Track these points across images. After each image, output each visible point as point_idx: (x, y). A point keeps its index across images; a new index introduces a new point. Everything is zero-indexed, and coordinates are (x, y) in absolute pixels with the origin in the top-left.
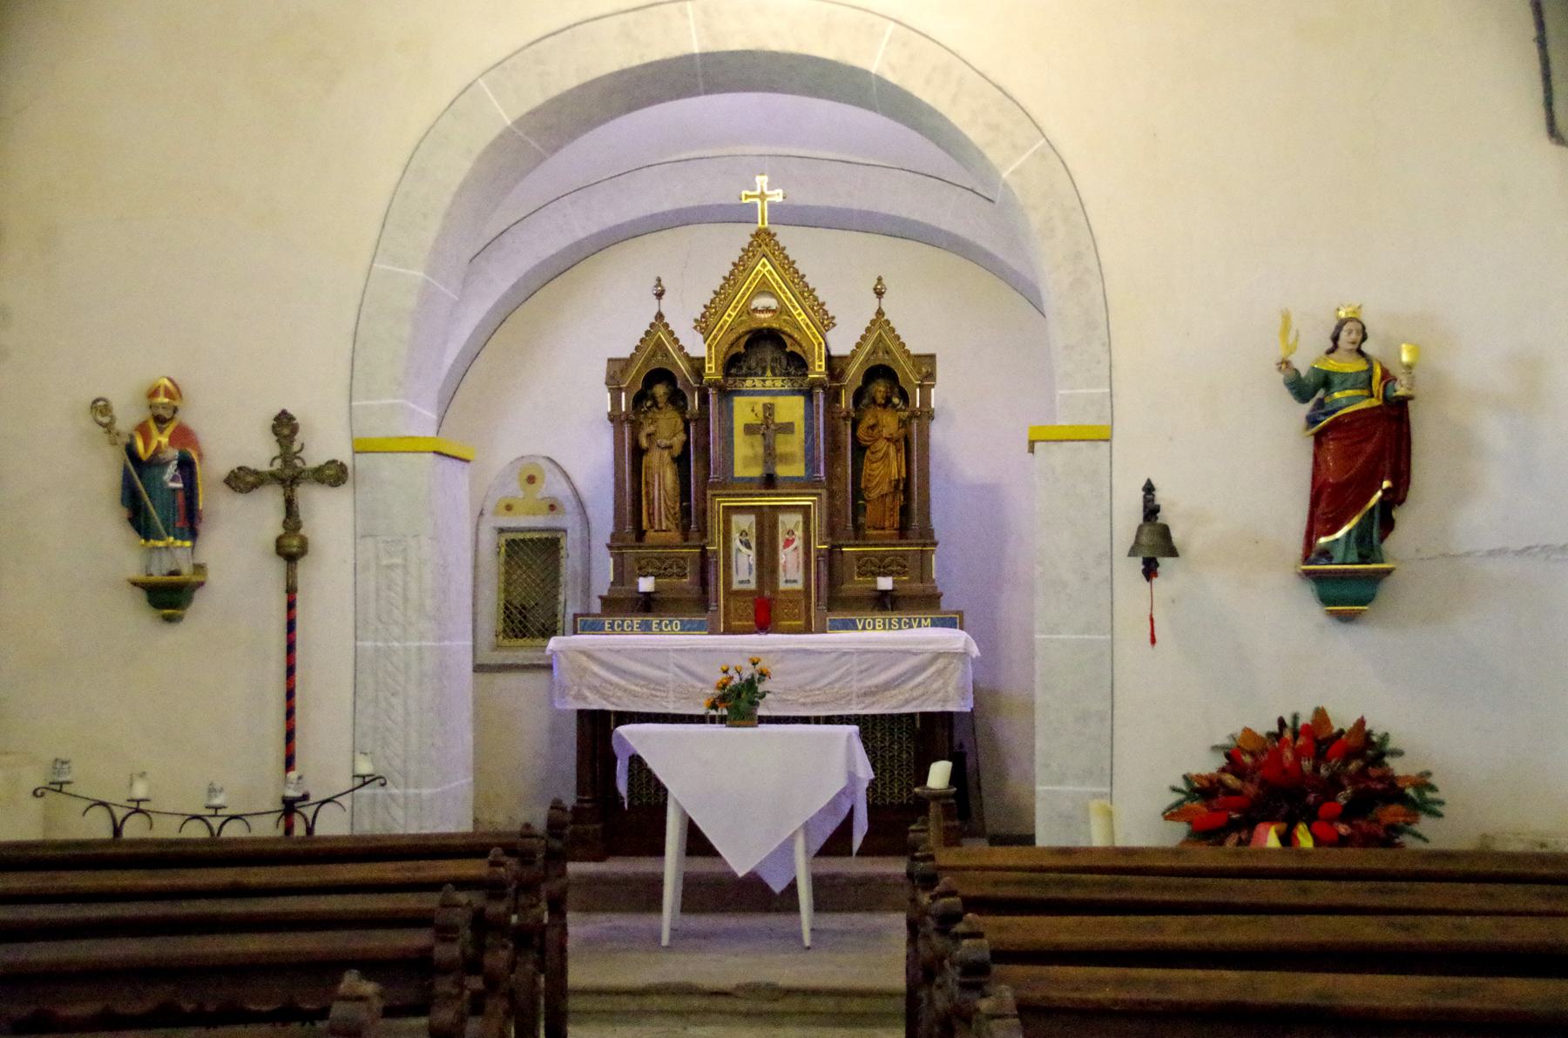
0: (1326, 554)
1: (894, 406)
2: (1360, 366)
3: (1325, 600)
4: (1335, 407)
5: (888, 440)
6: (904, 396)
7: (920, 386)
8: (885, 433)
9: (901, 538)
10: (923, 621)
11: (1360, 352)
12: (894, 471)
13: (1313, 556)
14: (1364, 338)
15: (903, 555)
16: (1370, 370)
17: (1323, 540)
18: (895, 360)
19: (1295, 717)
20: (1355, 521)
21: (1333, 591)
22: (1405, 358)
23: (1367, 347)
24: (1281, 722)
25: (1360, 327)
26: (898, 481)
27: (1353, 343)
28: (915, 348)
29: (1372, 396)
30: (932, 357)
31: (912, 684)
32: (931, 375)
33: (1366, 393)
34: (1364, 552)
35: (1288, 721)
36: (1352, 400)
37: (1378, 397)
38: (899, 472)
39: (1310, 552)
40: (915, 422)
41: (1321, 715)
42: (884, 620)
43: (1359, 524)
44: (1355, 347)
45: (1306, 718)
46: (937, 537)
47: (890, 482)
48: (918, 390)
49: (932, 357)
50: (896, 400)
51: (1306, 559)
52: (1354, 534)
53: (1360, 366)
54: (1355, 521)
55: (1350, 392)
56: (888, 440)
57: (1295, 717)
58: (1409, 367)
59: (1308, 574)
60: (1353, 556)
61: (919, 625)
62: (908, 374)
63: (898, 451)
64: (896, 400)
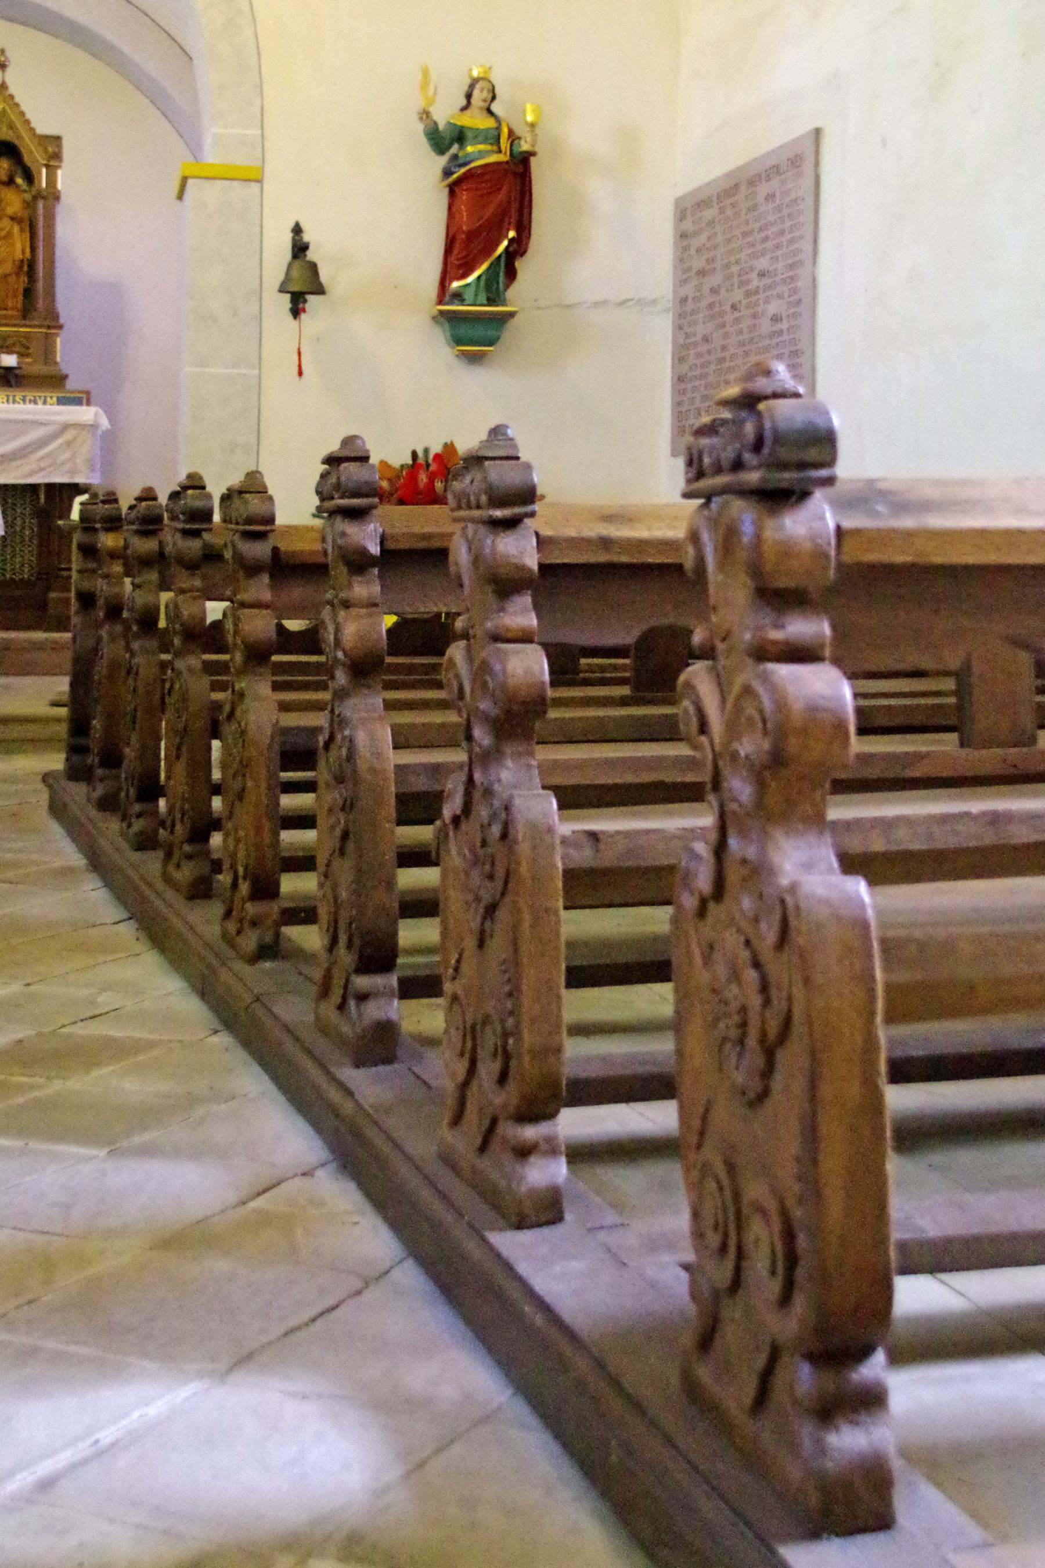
0: (458, 296)
1: (18, 186)
2: (490, 123)
3: (458, 341)
4: (468, 159)
5: (12, 219)
6: (29, 177)
7: (47, 166)
8: (10, 211)
9: (24, 318)
10: (49, 399)
11: (489, 112)
12: (18, 246)
13: (447, 298)
14: (494, 98)
15: (28, 336)
16: (499, 128)
17: (455, 284)
18: (19, 137)
19: (426, 451)
20: (484, 267)
21: (464, 330)
22: (530, 118)
23: (495, 107)
24: (414, 455)
25: (491, 88)
26: (22, 261)
27: (485, 101)
28: (43, 128)
29: (500, 151)
30: (58, 139)
31: (41, 453)
32: (57, 156)
33: (495, 148)
34: (492, 296)
35: (420, 454)
36: (482, 154)
37: (506, 153)
38: (23, 252)
39: (443, 293)
40: (41, 204)
41: (449, 448)
42: (8, 396)
43: (489, 268)
44: (487, 104)
45: (436, 448)
46: (62, 321)
47: (14, 261)
48: (44, 171)
49: (58, 139)
50: (19, 181)
51: (440, 301)
52: (483, 278)
53: (490, 123)
54: (484, 267)
55: (481, 147)
56: (12, 219)
57: (426, 451)
58: (532, 126)
59: (442, 313)
60: (482, 298)
61: (45, 403)
62: (33, 155)
63: (22, 230)
64: (19, 181)
